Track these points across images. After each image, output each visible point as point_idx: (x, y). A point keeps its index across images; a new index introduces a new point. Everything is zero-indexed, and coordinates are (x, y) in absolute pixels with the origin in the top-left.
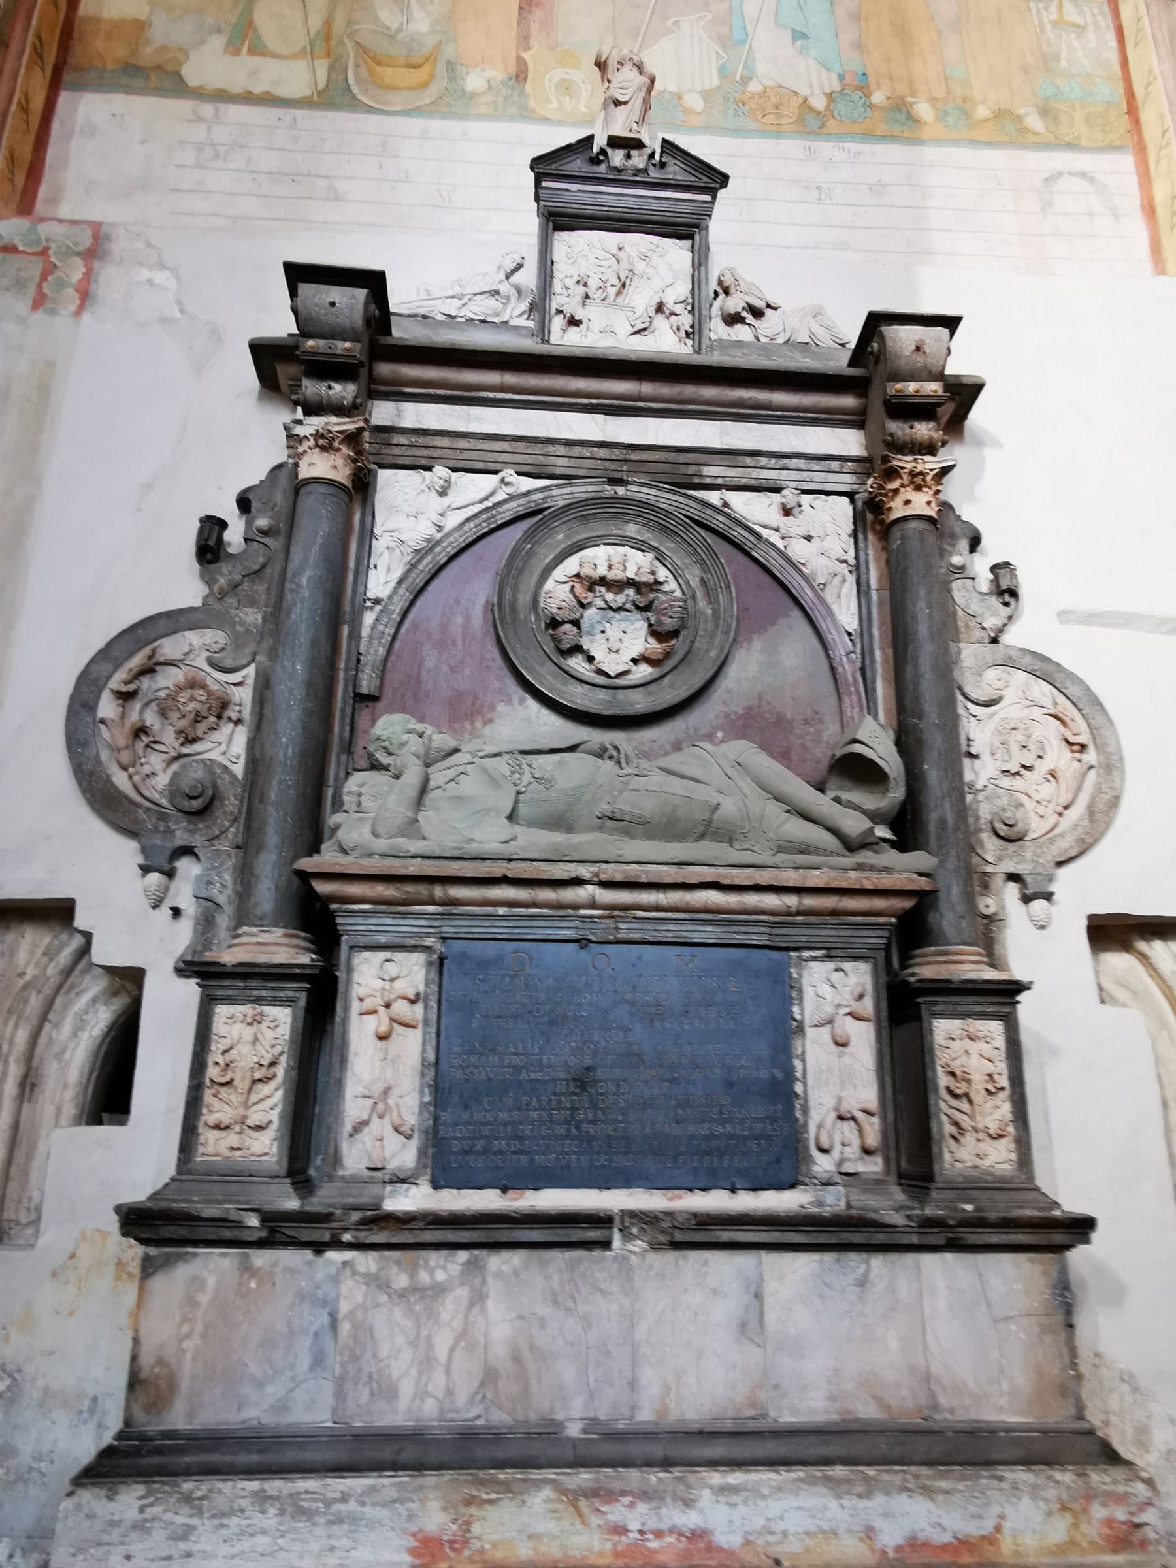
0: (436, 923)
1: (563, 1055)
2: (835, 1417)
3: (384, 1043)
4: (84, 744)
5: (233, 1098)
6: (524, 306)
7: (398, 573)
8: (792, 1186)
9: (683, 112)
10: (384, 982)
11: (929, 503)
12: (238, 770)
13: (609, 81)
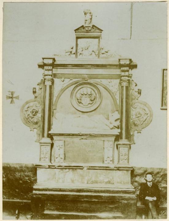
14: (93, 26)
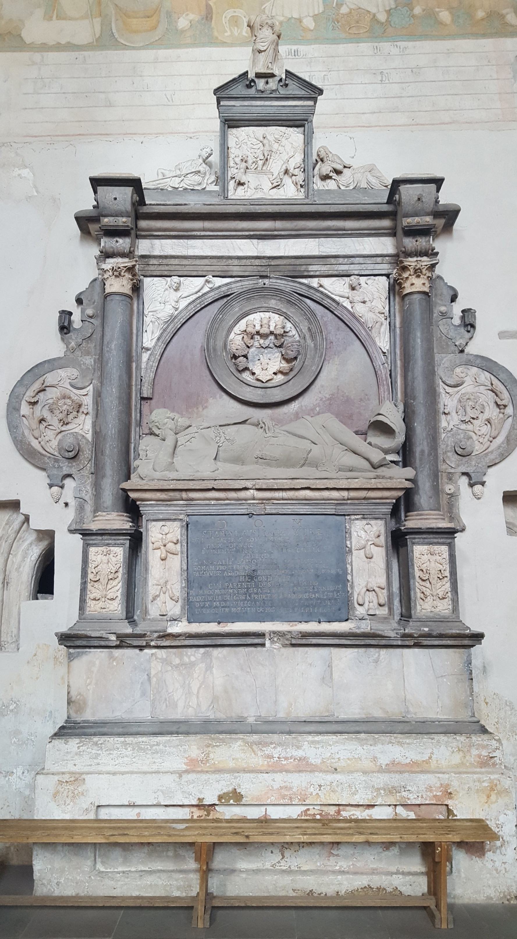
0: (184, 509)
1: (242, 566)
2: (364, 716)
3: (164, 561)
4: (16, 427)
5: (100, 587)
6: (213, 178)
7: (157, 334)
8: (347, 620)
9: (302, 30)
10: (161, 534)
11: (424, 284)
12: (89, 436)
13: (256, 36)
14: (288, 73)
